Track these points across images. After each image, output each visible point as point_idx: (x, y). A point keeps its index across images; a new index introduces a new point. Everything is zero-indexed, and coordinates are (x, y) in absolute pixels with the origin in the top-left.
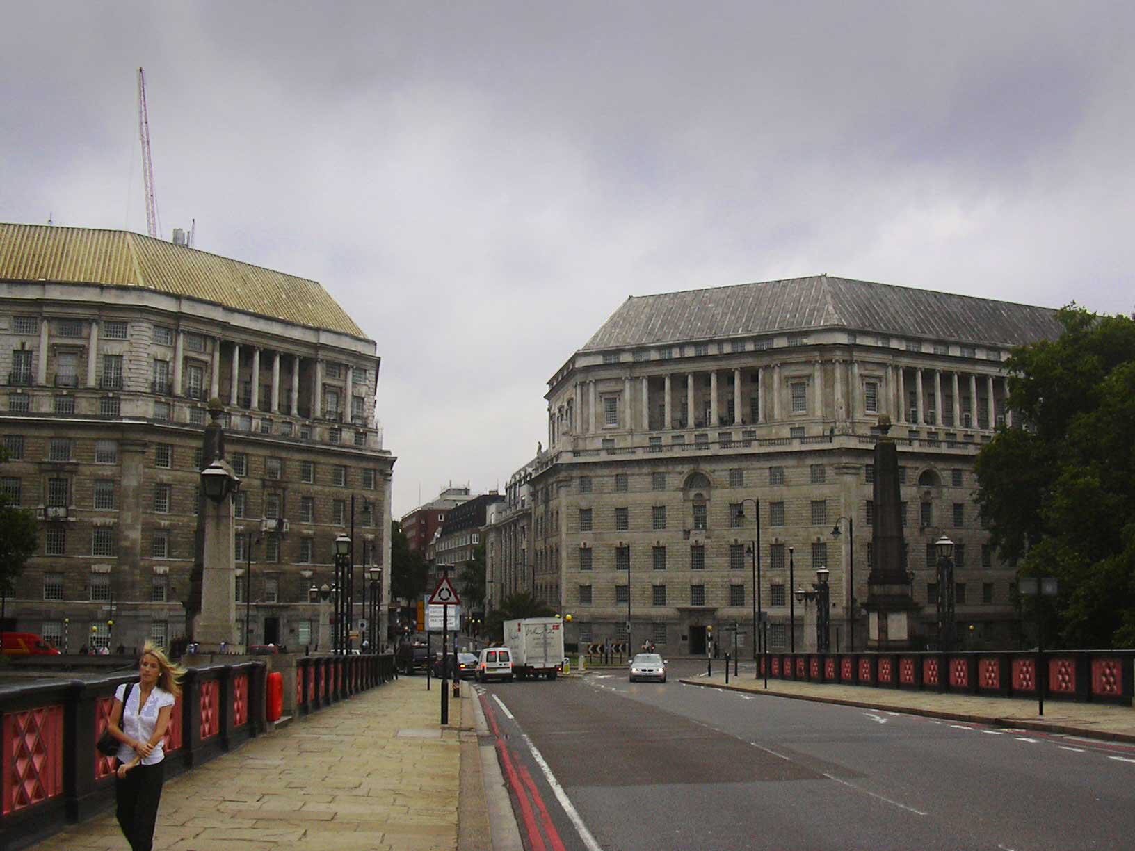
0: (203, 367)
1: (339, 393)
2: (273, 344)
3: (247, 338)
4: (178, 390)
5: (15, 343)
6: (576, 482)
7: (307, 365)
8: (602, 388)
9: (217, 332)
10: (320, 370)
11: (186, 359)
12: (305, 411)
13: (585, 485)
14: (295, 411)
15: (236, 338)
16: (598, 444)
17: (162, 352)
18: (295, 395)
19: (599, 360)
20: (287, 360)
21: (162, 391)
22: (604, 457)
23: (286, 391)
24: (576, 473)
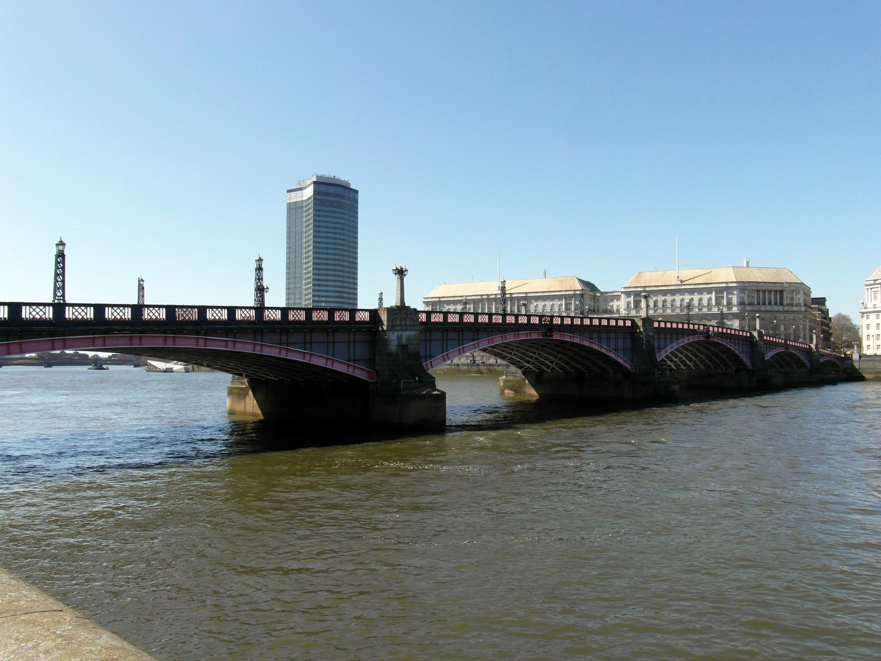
0: (753, 297)
1: (792, 298)
2: (771, 288)
3: (764, 288)
4: (746, 303)
5: (708, 296)
6: (866, 317)
7: (781, 292)
8: (873, 290)
9: (755, 288)
10: (785, 293)
11: (748, 296)
12: (781, 304)
13: (868, 317)
14: (778, 304)
15: (760, 288)
16: (872, 306)
17: (743, 295)
18: (778, 300)
19: (872, 282)
20: (776, 291)
21: (741, 304)
22: (873, 310)
23: (776, 299)
24: (865, 315)
